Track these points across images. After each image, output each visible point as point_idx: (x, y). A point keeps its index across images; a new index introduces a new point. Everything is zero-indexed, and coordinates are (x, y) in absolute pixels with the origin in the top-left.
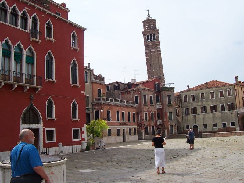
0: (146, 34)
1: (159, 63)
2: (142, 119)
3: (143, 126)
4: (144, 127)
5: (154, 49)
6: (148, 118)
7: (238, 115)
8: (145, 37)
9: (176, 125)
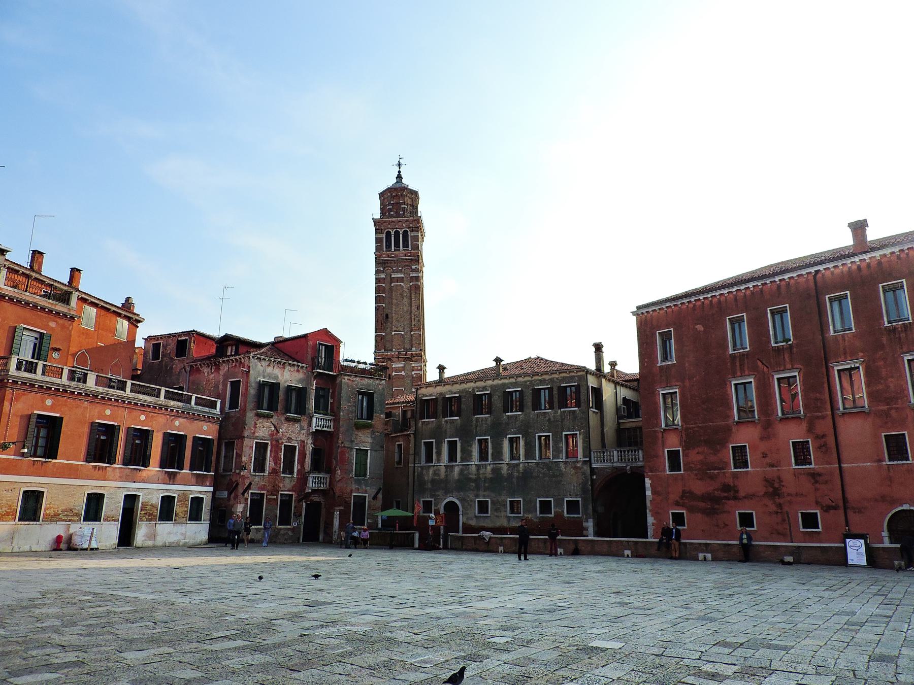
0: (382, 227)
1: (411, 312)
2: (241, 462)
3: (241, 490)
4: (243, 494)
5: (401, 271)
6: (269, 464)
7: (595, 477)
8: (380, 236)
9: (380, 496)
